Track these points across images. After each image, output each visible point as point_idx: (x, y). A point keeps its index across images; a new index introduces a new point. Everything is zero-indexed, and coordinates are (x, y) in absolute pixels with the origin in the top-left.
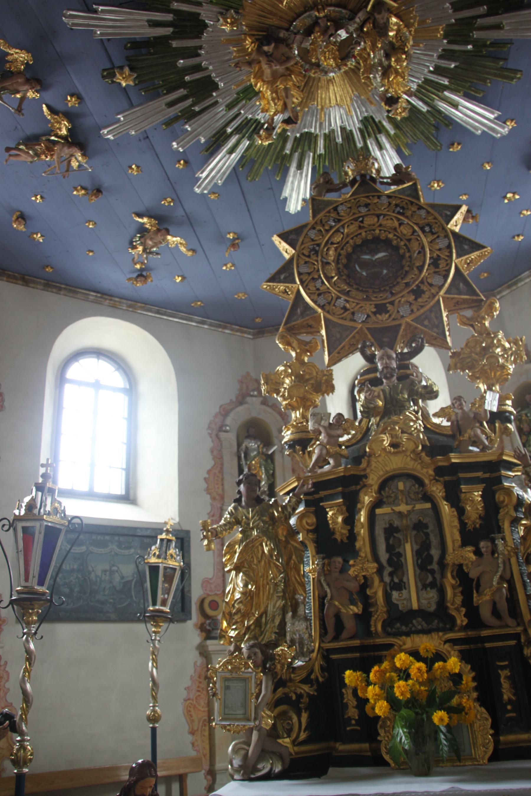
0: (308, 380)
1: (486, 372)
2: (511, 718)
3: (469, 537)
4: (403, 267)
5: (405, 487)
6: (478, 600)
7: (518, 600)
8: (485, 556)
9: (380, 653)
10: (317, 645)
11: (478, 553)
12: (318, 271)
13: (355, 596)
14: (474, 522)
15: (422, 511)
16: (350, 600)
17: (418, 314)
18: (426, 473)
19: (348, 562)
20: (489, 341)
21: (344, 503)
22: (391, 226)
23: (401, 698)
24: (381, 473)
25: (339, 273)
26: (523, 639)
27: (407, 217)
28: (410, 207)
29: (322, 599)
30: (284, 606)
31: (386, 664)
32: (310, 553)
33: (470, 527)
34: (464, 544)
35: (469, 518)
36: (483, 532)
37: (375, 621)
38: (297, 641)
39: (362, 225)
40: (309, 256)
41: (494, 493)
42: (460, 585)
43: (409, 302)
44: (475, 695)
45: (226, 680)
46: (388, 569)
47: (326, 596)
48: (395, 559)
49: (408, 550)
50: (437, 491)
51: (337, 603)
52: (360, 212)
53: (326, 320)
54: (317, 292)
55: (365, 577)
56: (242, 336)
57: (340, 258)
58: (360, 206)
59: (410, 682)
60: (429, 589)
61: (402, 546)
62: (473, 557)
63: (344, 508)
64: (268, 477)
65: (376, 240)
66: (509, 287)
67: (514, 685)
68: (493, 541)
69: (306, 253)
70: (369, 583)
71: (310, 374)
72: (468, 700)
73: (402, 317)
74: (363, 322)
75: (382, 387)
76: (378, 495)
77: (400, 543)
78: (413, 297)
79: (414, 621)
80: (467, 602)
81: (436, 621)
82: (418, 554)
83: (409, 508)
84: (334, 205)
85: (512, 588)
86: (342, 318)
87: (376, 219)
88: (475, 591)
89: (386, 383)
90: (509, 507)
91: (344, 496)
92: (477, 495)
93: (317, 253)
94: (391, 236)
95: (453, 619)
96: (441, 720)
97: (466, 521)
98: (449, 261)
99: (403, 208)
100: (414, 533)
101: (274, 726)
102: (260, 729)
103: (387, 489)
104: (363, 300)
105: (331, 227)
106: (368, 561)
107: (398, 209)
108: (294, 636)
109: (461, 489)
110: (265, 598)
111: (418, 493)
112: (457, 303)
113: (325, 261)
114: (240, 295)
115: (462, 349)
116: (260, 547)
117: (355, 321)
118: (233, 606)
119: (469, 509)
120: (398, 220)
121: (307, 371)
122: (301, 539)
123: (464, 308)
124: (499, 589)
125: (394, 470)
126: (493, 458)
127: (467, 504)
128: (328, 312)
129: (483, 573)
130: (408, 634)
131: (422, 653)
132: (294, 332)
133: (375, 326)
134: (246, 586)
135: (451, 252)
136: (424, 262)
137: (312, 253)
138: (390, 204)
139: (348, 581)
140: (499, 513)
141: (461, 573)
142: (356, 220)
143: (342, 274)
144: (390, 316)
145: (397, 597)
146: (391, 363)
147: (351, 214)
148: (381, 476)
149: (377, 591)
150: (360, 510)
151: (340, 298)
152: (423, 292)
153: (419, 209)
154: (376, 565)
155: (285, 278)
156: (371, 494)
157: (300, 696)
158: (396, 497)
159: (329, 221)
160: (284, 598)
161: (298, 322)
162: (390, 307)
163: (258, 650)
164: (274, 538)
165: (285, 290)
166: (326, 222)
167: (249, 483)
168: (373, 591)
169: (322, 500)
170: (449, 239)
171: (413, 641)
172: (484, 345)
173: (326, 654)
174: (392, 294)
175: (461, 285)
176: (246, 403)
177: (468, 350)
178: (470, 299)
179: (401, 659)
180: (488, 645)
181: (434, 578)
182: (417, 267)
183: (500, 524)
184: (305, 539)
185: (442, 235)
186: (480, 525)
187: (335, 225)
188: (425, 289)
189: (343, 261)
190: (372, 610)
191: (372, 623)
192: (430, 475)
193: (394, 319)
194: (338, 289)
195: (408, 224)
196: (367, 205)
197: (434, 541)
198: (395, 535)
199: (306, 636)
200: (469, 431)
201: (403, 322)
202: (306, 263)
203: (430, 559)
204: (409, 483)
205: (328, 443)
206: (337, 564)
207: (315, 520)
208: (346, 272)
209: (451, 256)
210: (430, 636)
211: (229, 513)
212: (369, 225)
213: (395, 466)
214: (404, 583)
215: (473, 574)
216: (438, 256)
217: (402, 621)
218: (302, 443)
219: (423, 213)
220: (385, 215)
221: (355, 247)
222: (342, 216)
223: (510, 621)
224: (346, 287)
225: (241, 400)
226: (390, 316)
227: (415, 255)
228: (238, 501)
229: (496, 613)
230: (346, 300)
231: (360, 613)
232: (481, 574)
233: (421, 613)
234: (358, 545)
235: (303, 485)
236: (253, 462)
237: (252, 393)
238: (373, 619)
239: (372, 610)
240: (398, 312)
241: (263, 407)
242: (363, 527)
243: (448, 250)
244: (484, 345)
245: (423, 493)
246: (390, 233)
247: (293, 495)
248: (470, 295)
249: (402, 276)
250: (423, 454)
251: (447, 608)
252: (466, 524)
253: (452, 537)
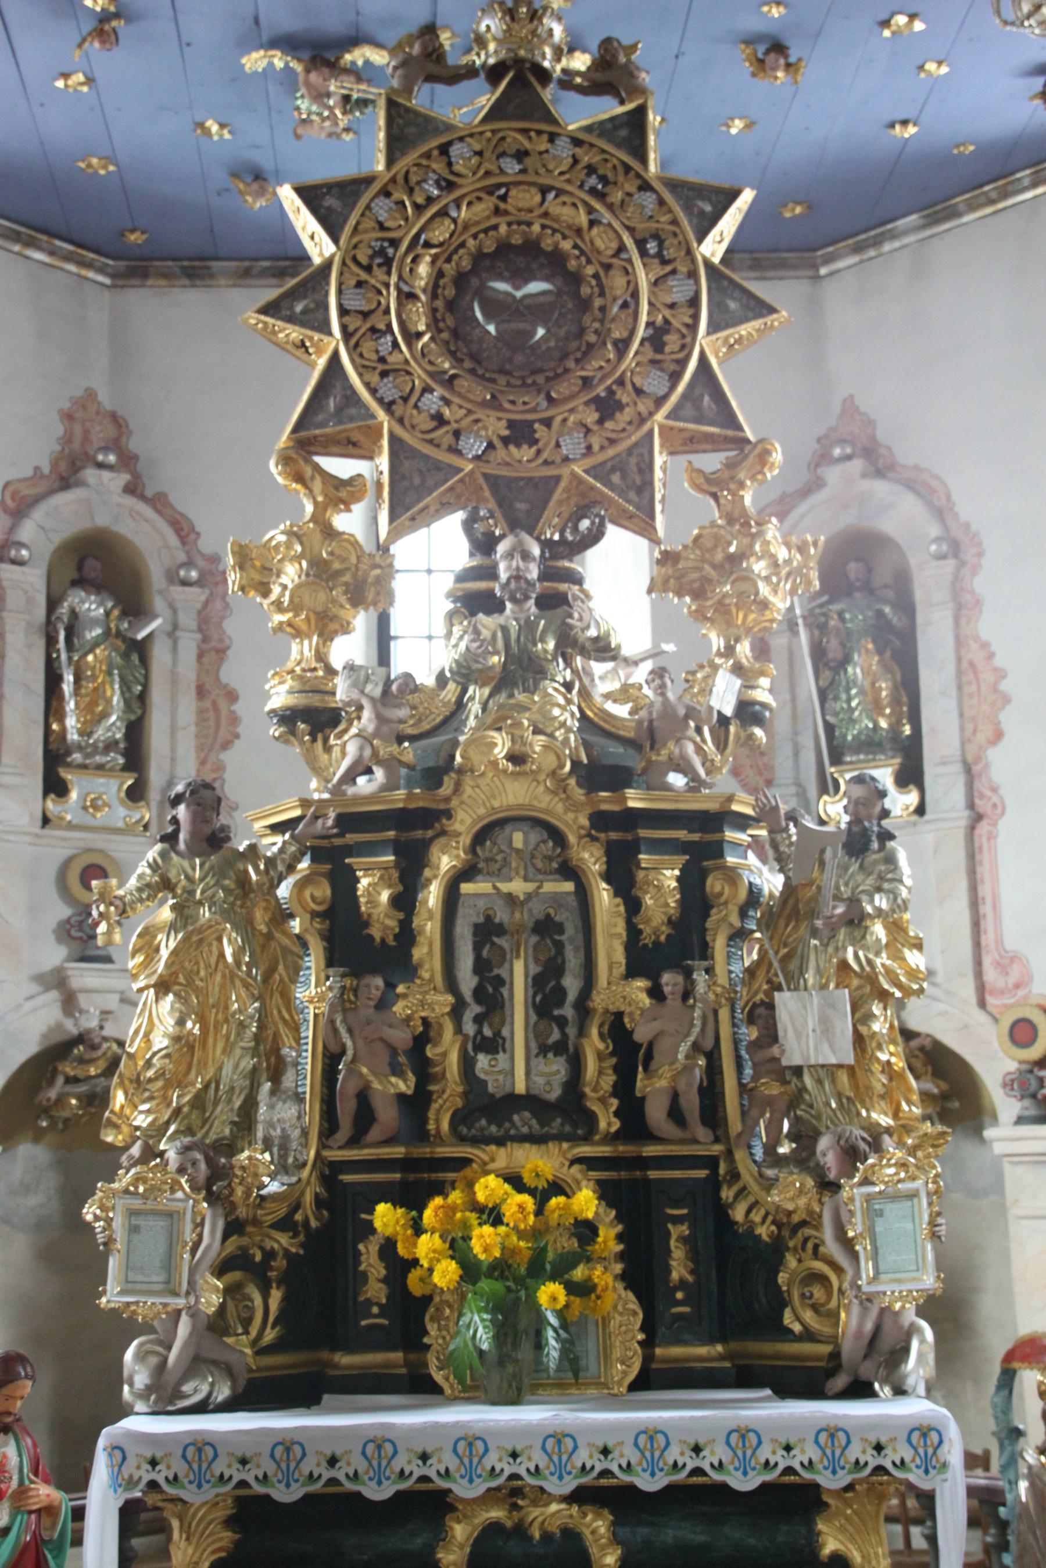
0: (339, 573)
1: (728, 612)
2: (680, 1316)
3: (643, 960)
4: (582, 331)
5: (526, 842)
6: (646, 1086)
7: (723, 1093)
8: (668, 1001)
9: (441, 1176)
10: (312, 1153)
11: (656, 993)
12: (387, 311)
13: (402, 1059)
14: (656, 931)
15: (556, 899)
16: (391, 1064)
17: (600, 458)
18: (573, 822)
19: (394, 987)
20: (746, 541)
21: (397, 864)
22: (571, 222)
23: (482, 1257)
24: (482, 811)
25: (435, 323)
26: (722, 1169)
27: (610, 207)
28: (621, 179)
29: (331, 1060)
30: (255, 1069)
31: (456, 1196)
32: (313, 961)
33: (647, 938)
34: (631, 973)
35: (648, 921)
36: (669, 953)
37: (438, 1111)
38: (276, 1142)
39: (502, 206)
40: (368, 269)
41: (704, 874)
42: (613, 1054)
43: (585, 426)
44: (618, 1268)
45: (132, 1213)
46: (474, 1009)
47: (343, 1052)
48: (490, 990)
49: (519, 974)
50: (592, 860)
51: (365, 1070)
52: (502, 172)
53: (393, 439)
54: (381, 367)
55: (425, 1021)
56: (79, 276)
57: (442, 282)
58: (503, 154)
59: (502, 1229)
60: (550, 1055)
61: (507, 965)
62: (646, 1001)
63: (395, 874)
64: (127, 702)
65: (531, 247)
66: (858, 249)
67: (694, 1255)
68: (688, 973)
69: (364, 260)
70: (432, 1034)
71: (343, 560)
72: (604, 1276)
73: (566, 459)
74: (477, 458)
75: (501, 620)
76: (470, 857)
77: (502, 956)
78: (596, 416)
79: (516, 1117)
80: (624, 1087)
81: (559, 1120)
82: (537, 983)
83: (530, 887)
84: (443, 139)
85: (714, 1070)
86: (431, 442)
87: (538, 198)
88: (640, 1069)
89: (513, 612)
90: (730, 906)
91: (400, 849)
92: (670, 877)
93: (388, 263)
94: (566, 245)
95: (591, 1119)
96: (554, 1299)
97: (641, 927)
98: (688, 340)
99: (604, 179)
100: (534, 939)
101: (222, 1308)
102: (194, 1313)
103: (488, 843)
104: (484, 404)
105: (430, 200)
106: (435, 989)
107: (593, 181)
108: (272, 1132)
109: (638, 862)
110: (219, 1051)
111: (550, 859)
112: (691, 440)
113: (406, 288)
114: (95, 161)
115: (685, 547)
116: (215, 943)
117: (458, 452)
118: (149, 1064)
119: (649, 902)
120: (590, 210)
121: (337, 552)
122: (297, 931)
123: (705, 451)
124: (688, 1069)
125: (510, 808)
126: (712, 806)
127: (647, 893)
128: (401, 421)
129: (660, 1034)
130: (500, 1142)
131: (528, 1179)
132: (312, 449)
133: (504, 472)
134: (181, 1022)
135: (696, 317)
136: (632, 332)
137: (378, 261)
138: (576, 161)
139: (391, 1026)
140: (708, 915)
141: (618, 1030)
142: (490, 190)
143: (441, 325)
144: (539, 452)
145: (486, 1067)
146: (527, 569)
147: (481, 172)
148: (480, 818)
149: (448, 1052)
150: (429, 882)
151: (431, 391)
152: (620, 407)
153: (641, 189)
154: (450, 999)
155: (305, 312)
156: (455, 852)
157: (269, 1255)
158: (506, 862)
159: (425, 181)
160: (255, 1052)
161: (328, 430)
162: (540, 431)
163: (199, 1156)
164: (246, 927)
165: (303, 341)
166: (418, 183)
167: (199, 805)
168: (439, 1050)
169: (350, 850)
170: (697, 283)
171: (510, 1156)
172: (732, 549)
173: (330, 1173)
174: (550, 400)
175: (706, 399)
176: (81, 484)
177: (698, 552)
178: (719, 436)
179: (489, 1187)
180: (653, 1174)
181: (564, 1034)
182: (615, 343)
183: (708, 938)
184: (306, 930)
185: (683, 269)
186: (669, 936)
187: (439, 197)
188: (625, 399)
189: (446, 292)
190: (432, 1088)
191: (431, 1114)
192: (582, 827)
193: (546, 463)
194: (429, 368)
195: (610, 225)
196: (521, 155)
197: (573, 959)
198: (495, 939)
199: (296, 1133)
200: (671, 745)
201: (565, 471)
202: (360, 284)
203: (560, 993)
204: (535, 836)
205: (377, 734)
206: (373, 991)
207: (328, 892)
208: (450, 321)
209: (693, 327)
210: (543, 1147)
211: (150, 866)
212: (520, 210)
213: (512, 800)
214: (504, 1039)
215: (642, 1034)
216: (666, 321)
217: (491, 1114)
218: (314, 720)
219: (648, 200)
220: (560, 192)
221: (479, 257)
222: (458, 175)
223: (702, 1133)
224: (447, 365)
225: (67, 473)
226: (539, 452)
227: (615, 309)
228: (170, 839)
229: (676, 1113)
230: (443, 398)
231: (410, 1092)
232: (655, 1037)
233: (531, 1102)
234: (418, 953)
235: (316, 818)
236: (90, 658)
237: (100, 457)
238: (435, 1106)
239: (432, 1088)
240: (558, 445)
241: (130, 501)
242: (431, 918)
243: (691, 311)
244: (732, 549)
245: (560, 859)
246: (565, 237)
247: (292, 836)
248: (721, 426)
249: (579, 355)
250: (572, 782)
251: (582, 1096)
252: (640, 932)
253: (609, 956)
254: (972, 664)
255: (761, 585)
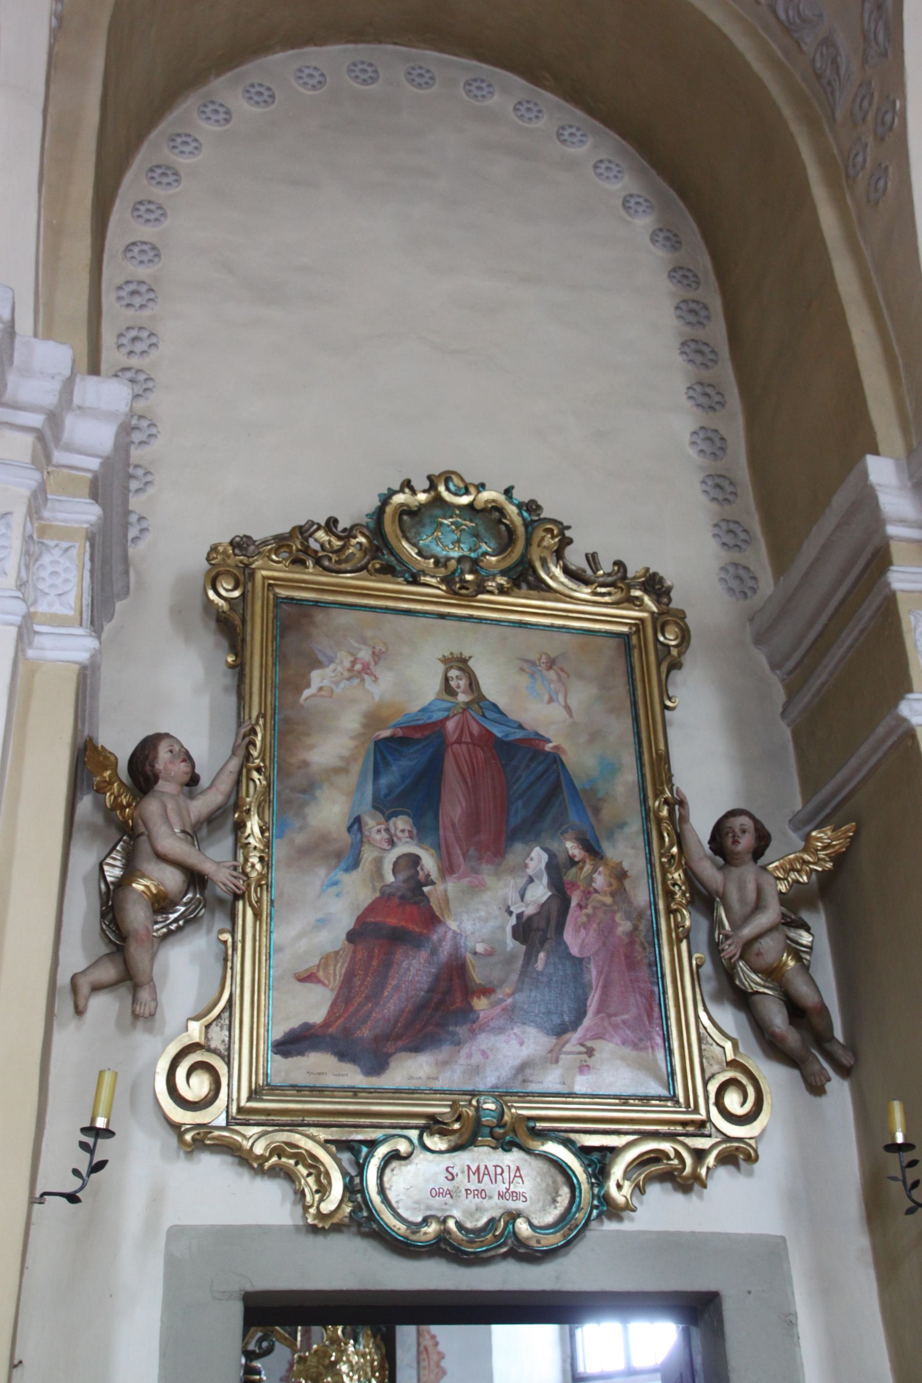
172: (333, 1359)
244: (333, 1359)
254: (426, 1349)
255: (345, 1376)
